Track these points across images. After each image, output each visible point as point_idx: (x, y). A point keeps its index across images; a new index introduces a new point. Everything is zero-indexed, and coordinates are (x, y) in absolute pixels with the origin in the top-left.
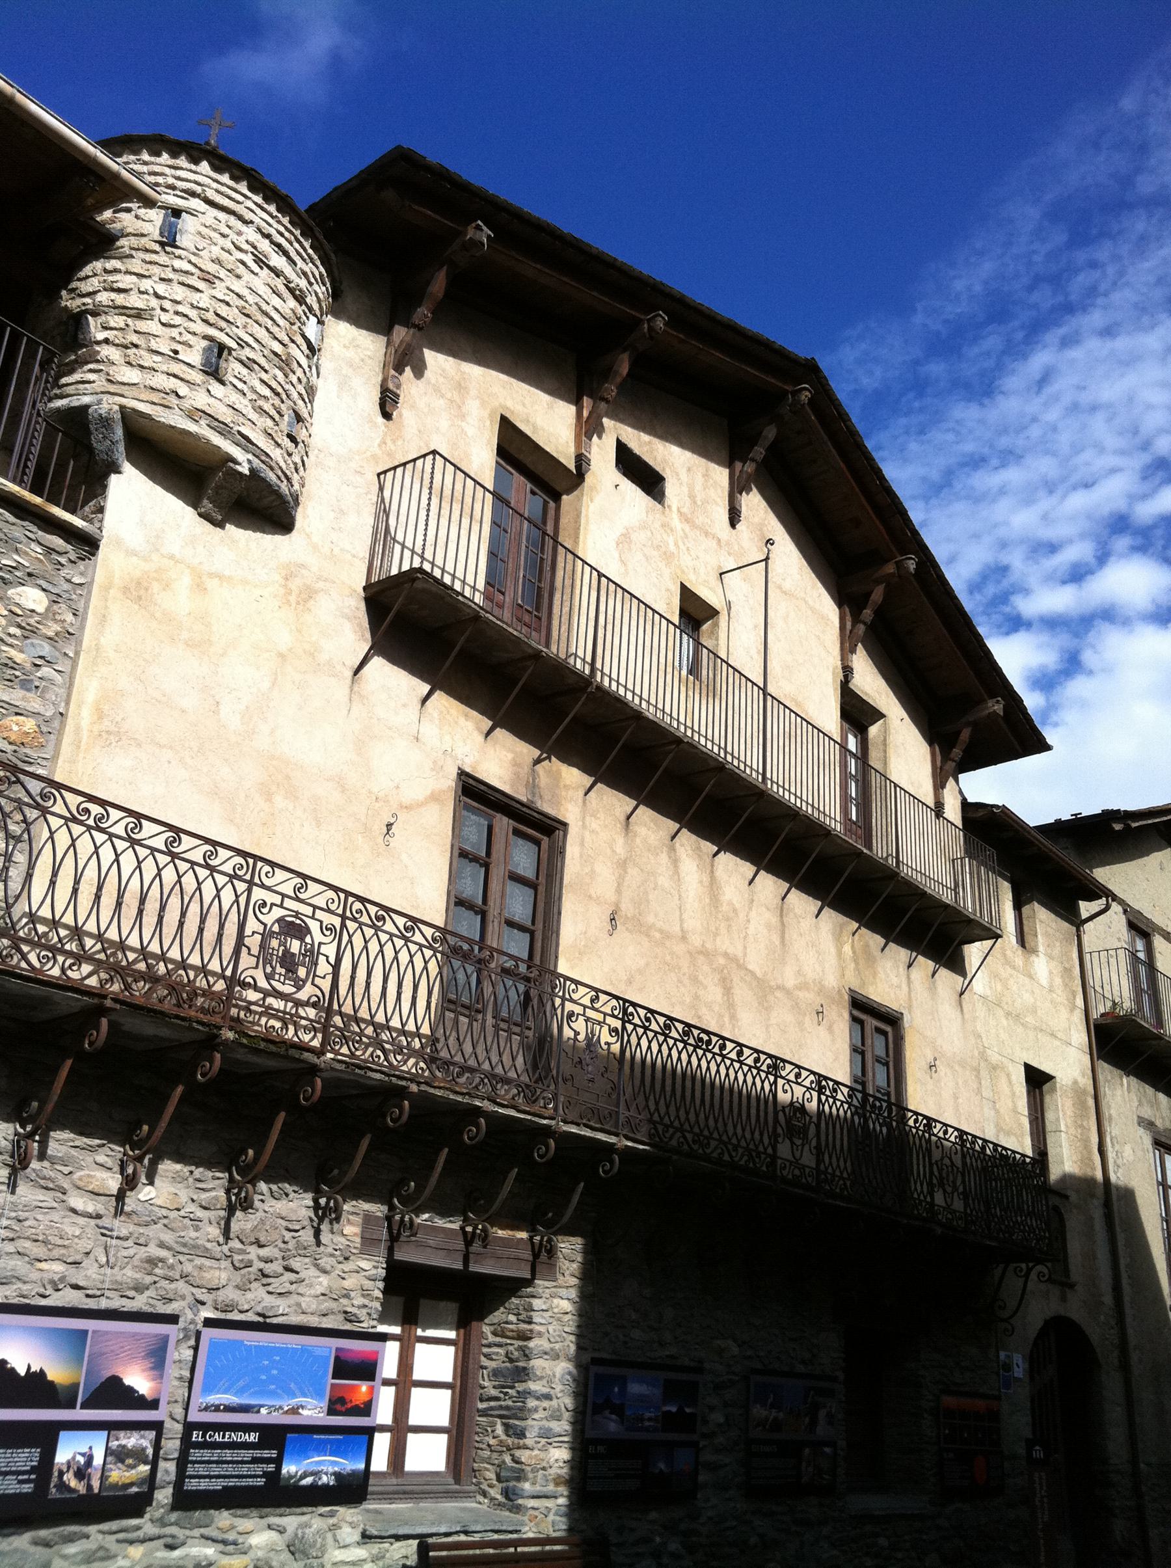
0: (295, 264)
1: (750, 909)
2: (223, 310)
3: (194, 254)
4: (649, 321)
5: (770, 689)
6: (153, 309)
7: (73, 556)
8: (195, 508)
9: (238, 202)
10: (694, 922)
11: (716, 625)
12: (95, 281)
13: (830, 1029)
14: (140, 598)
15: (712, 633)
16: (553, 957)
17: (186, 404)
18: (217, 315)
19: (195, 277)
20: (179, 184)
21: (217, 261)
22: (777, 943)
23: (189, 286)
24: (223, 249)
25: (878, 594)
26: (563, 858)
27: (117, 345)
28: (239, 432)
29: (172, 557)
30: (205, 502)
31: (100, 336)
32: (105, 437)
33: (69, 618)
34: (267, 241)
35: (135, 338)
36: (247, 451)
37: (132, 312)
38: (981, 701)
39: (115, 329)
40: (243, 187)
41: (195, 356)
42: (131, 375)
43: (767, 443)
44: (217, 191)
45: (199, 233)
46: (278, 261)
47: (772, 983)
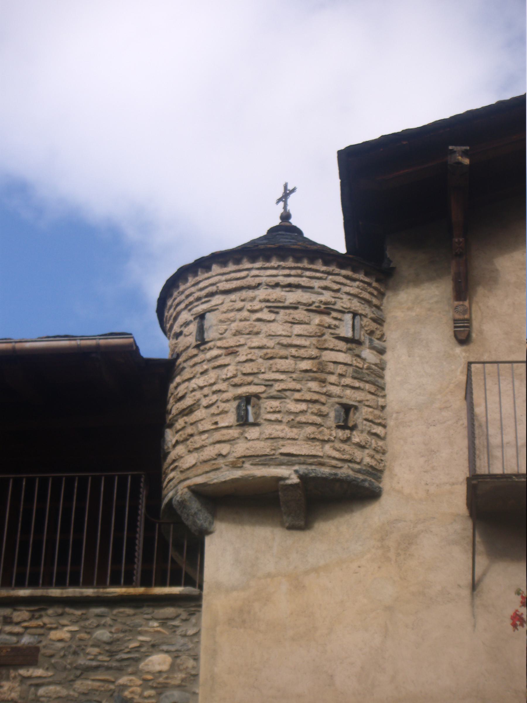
0: (312, 288)
2: (248, 368)
3: (220, 339)
7: (184, 616)
9: (244, 278)
14: (244, 622)
17: (231, 459)
18: (245, 374)
21: (238, 333)
24: (241, 320)
28: (282, 454)
29: (269, 575)
33: (191, 663)
34: (278, 290)
36: (293, 464)
37: (187, 411)
40: (247, 265)
41: (231, 419)
44: (227, 281)
45: (221, 321)
46: (292, 297)
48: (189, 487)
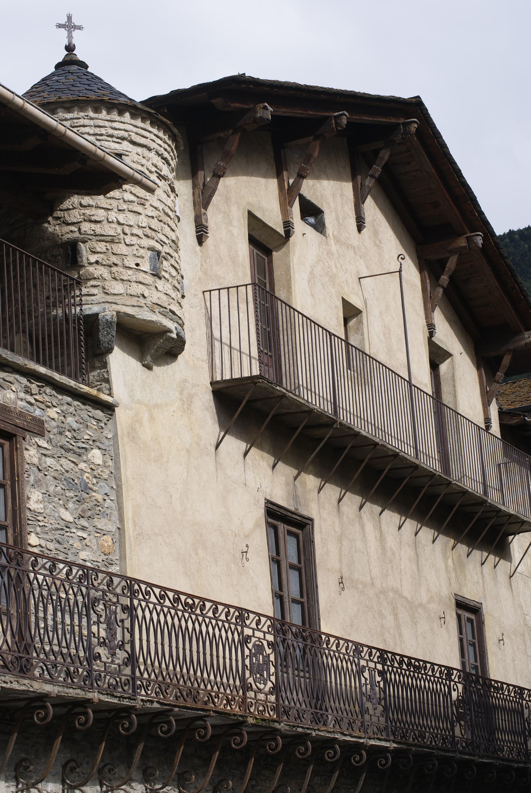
1: (401, 549)
4: (336, 117)
5: (413, 382)
6: (119, 234)
8: (141, 362)
10: (376, 572)
11: (360, 322)
12: (75, 212)
13: (447, 629)
15: (358, 328)
16: (317, 620)
19: (136, 204)
20: (116, 133)
22: (416, 571)
23: (134, 212)
25: (452, 263)
26: (314, 545)
27: (105, 265)
30: (149, 358)
31: (93, 258)
32: (108, 333)
35: (114, 259)
37: (109, 239)
38: (519, 332)
39: (101, 253)
42: (118, 288)
43: (383, 163)
47: (416, 603)
48: (118, 313)
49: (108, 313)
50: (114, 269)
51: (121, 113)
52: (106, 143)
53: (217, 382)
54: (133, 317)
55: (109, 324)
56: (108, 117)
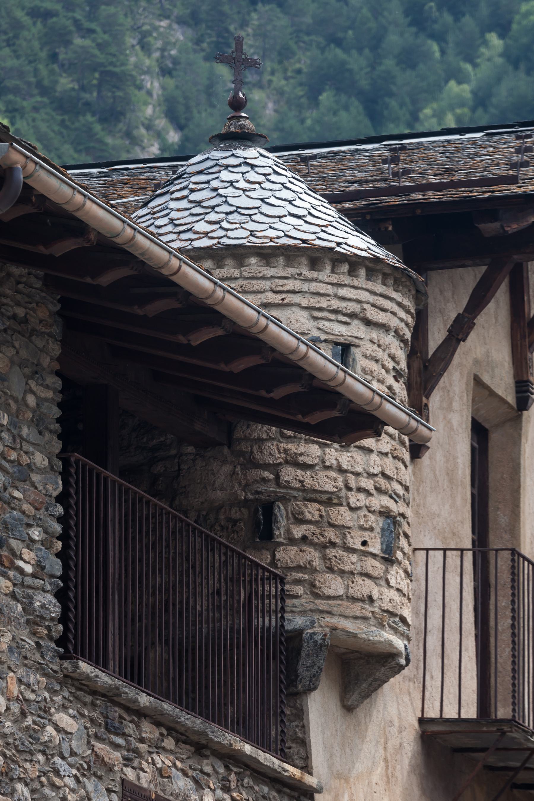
6: (340, 490)
31: (298, 532)
35: (331, 534)
37: (325, 497)
48: (334, 629)
49: (317, 629)
50: (331, 552)
51: (352, 273)
52: (327, 324)
53: (432, 721)
54: (355, 636)
55: (319, 647)
56: (334, 279)
